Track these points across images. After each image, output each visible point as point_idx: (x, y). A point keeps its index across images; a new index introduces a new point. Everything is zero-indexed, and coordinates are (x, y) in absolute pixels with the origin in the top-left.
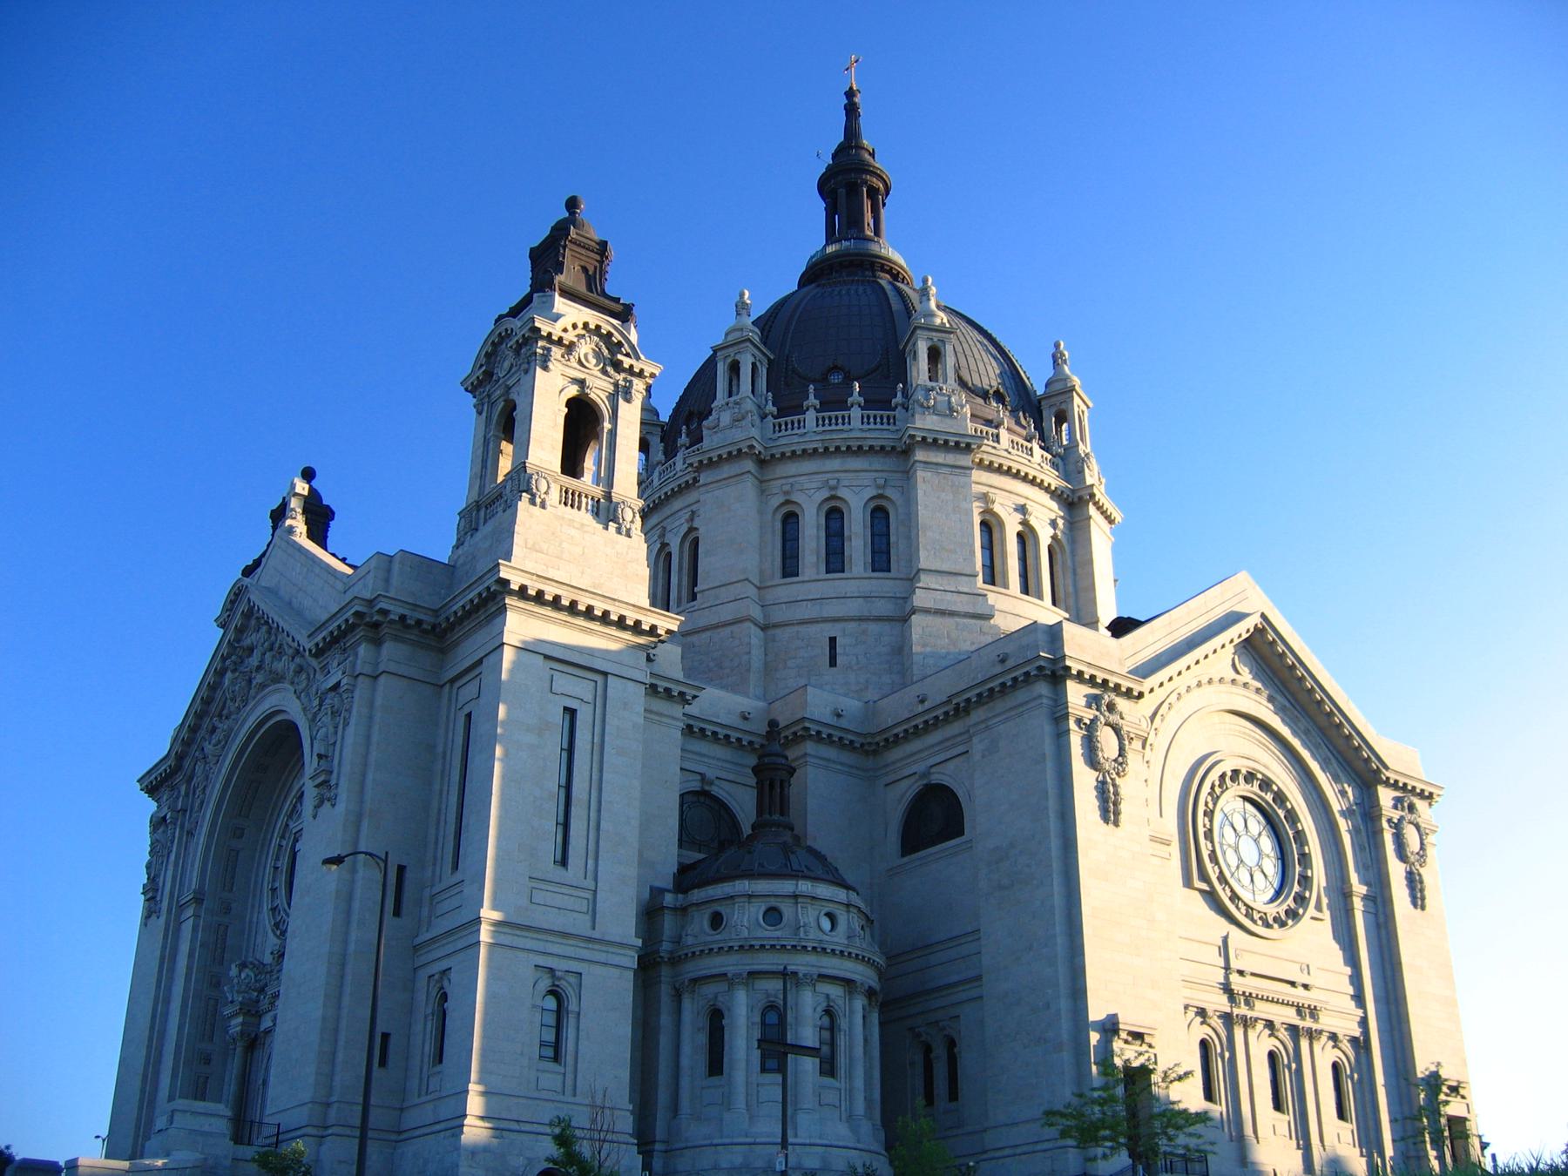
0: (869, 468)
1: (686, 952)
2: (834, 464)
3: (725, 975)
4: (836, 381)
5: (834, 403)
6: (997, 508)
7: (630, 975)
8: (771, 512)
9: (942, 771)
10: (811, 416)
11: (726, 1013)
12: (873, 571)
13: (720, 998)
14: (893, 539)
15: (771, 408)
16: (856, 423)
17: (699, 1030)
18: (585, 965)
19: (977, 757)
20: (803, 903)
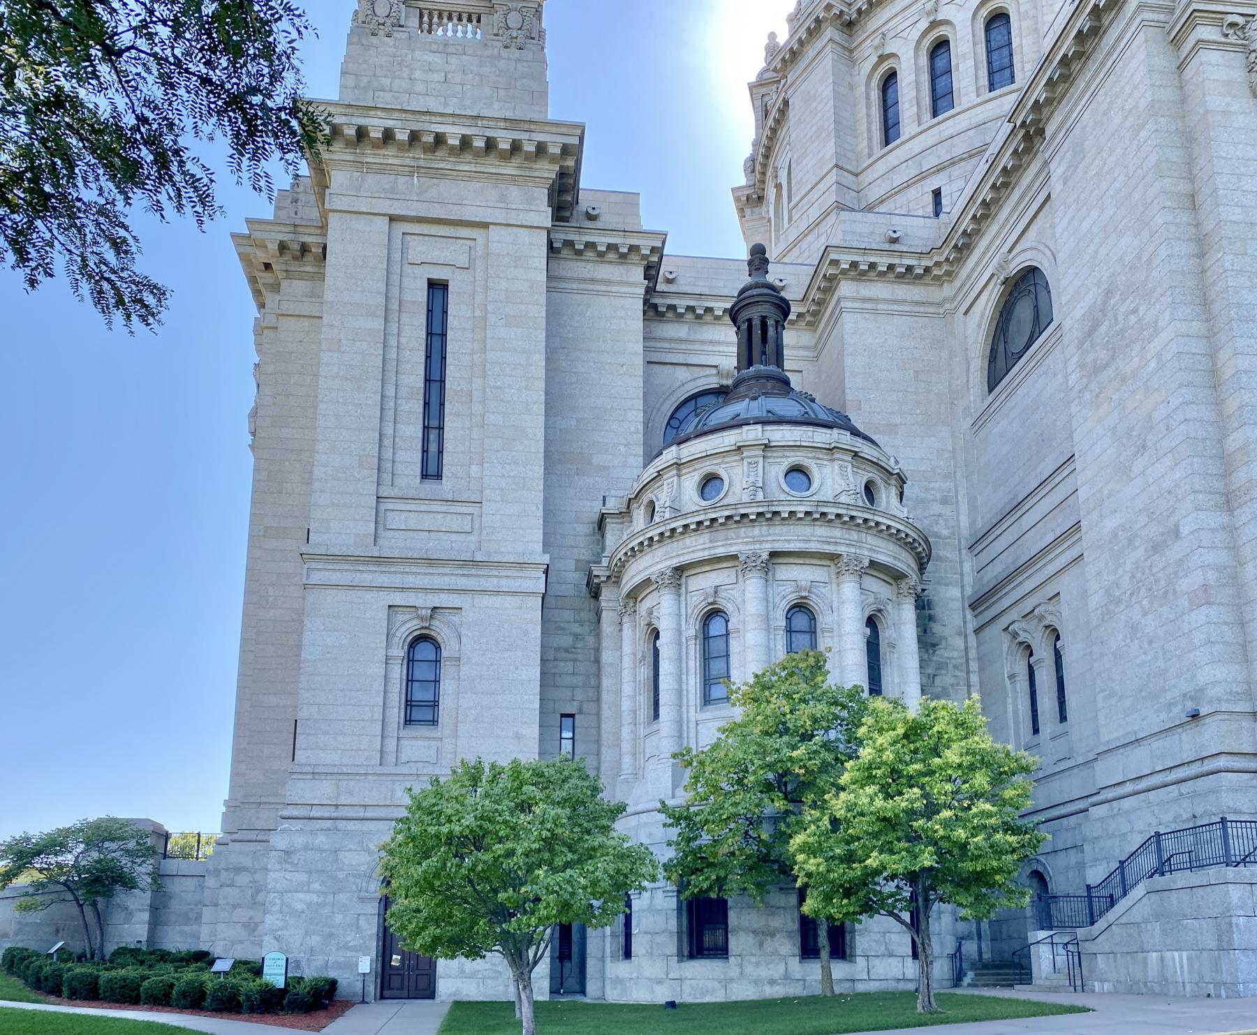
18: (468, 597)
20: (749, 457)
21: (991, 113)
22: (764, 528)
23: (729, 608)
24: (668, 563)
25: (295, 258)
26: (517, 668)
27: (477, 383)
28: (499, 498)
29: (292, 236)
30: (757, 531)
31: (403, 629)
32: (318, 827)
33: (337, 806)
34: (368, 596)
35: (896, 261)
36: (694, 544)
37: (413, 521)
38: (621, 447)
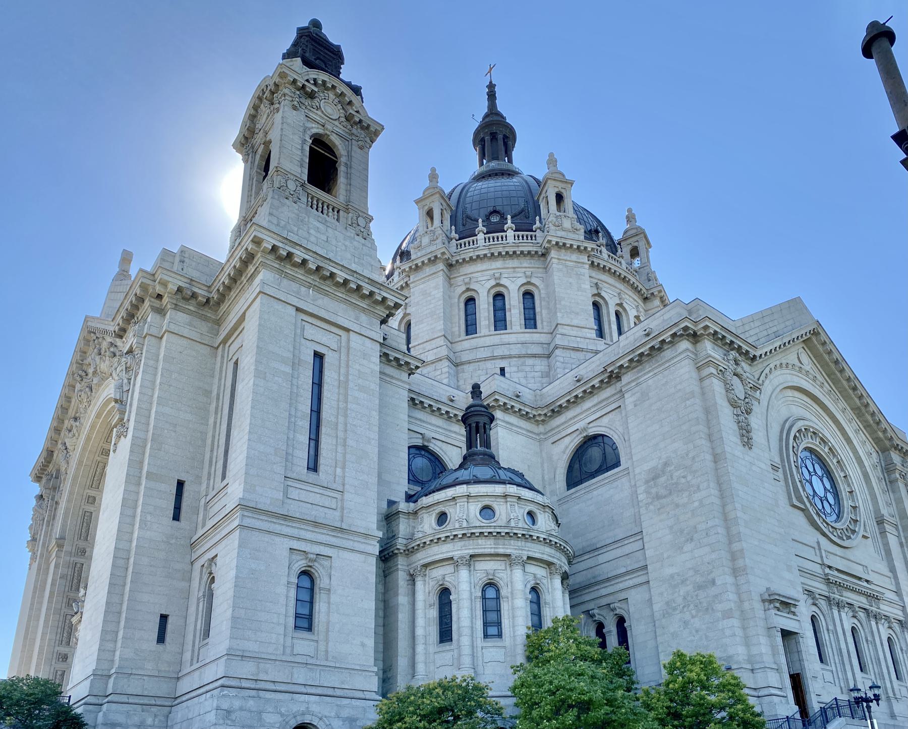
0: (520, 266)
1: (418, 543)
2: (499, 264)
3: (452, 558)
4: (495, 221)
5: (496, 229)
6: (603, 294)
7: (373, 561)
8: (457, 297)
9: (598, 424)
10: (481, 236)
11: (452, 590)
12: (526, 328)
13: (447, 579)
14: (538, 309)
15: (454, 235)
16: (511, 239)
17: (430, 606)
19: (630, 407)
20: (511, 502)
21: (528, 339)
22: (523, 543)
23: (501, 584)
24: (467, 551)
25: (184, 298)
26: (362, 601)
27: (341, 419)
28: (353, 492)
29: (187, 285)
30: (520, 543)
31: (296, 565)
32: (247, 694)
33: (256, 680)
34: (278, 539)
35: (522, 408)
36: (484, 543)
37: (303, 496)
38: (397, 472)
